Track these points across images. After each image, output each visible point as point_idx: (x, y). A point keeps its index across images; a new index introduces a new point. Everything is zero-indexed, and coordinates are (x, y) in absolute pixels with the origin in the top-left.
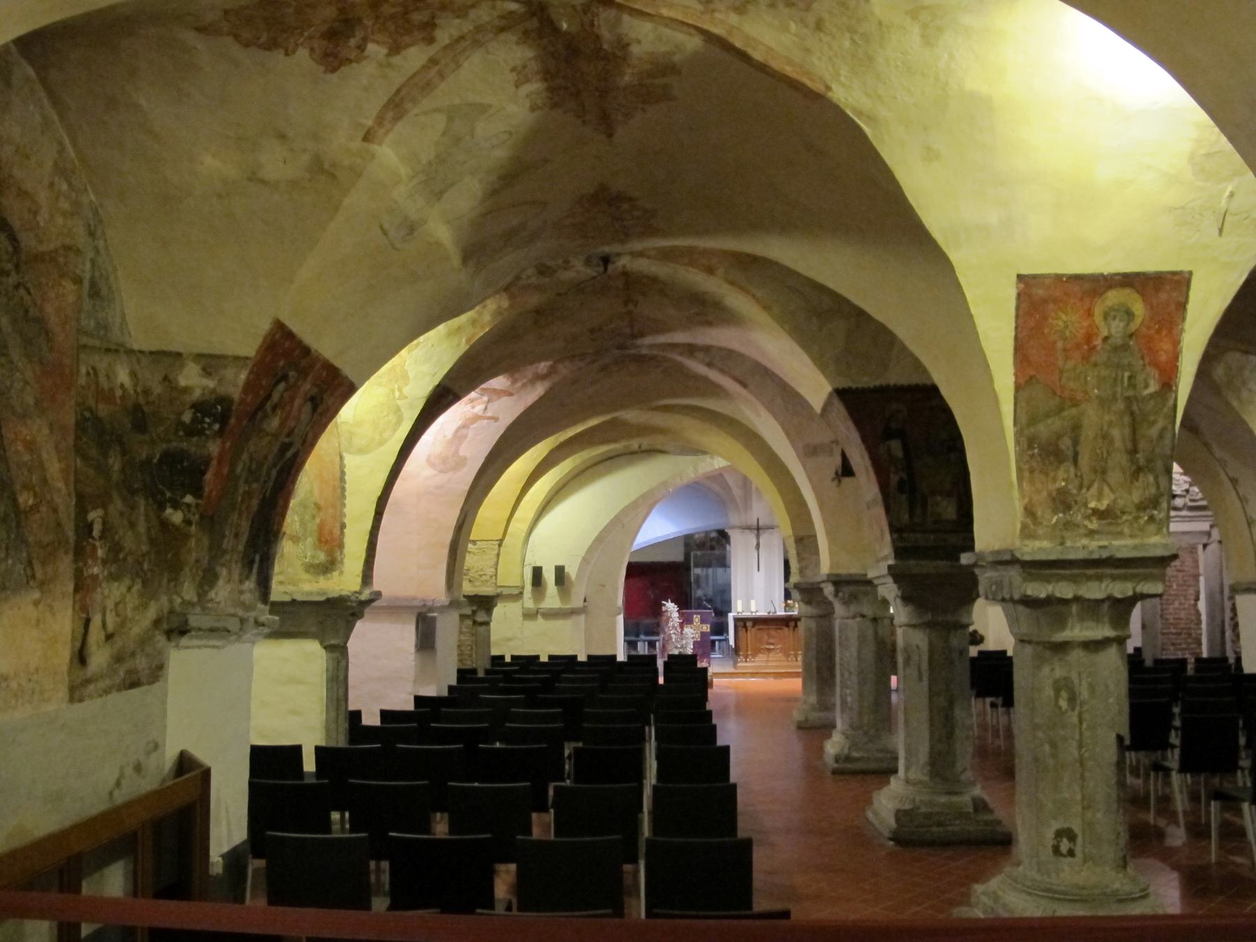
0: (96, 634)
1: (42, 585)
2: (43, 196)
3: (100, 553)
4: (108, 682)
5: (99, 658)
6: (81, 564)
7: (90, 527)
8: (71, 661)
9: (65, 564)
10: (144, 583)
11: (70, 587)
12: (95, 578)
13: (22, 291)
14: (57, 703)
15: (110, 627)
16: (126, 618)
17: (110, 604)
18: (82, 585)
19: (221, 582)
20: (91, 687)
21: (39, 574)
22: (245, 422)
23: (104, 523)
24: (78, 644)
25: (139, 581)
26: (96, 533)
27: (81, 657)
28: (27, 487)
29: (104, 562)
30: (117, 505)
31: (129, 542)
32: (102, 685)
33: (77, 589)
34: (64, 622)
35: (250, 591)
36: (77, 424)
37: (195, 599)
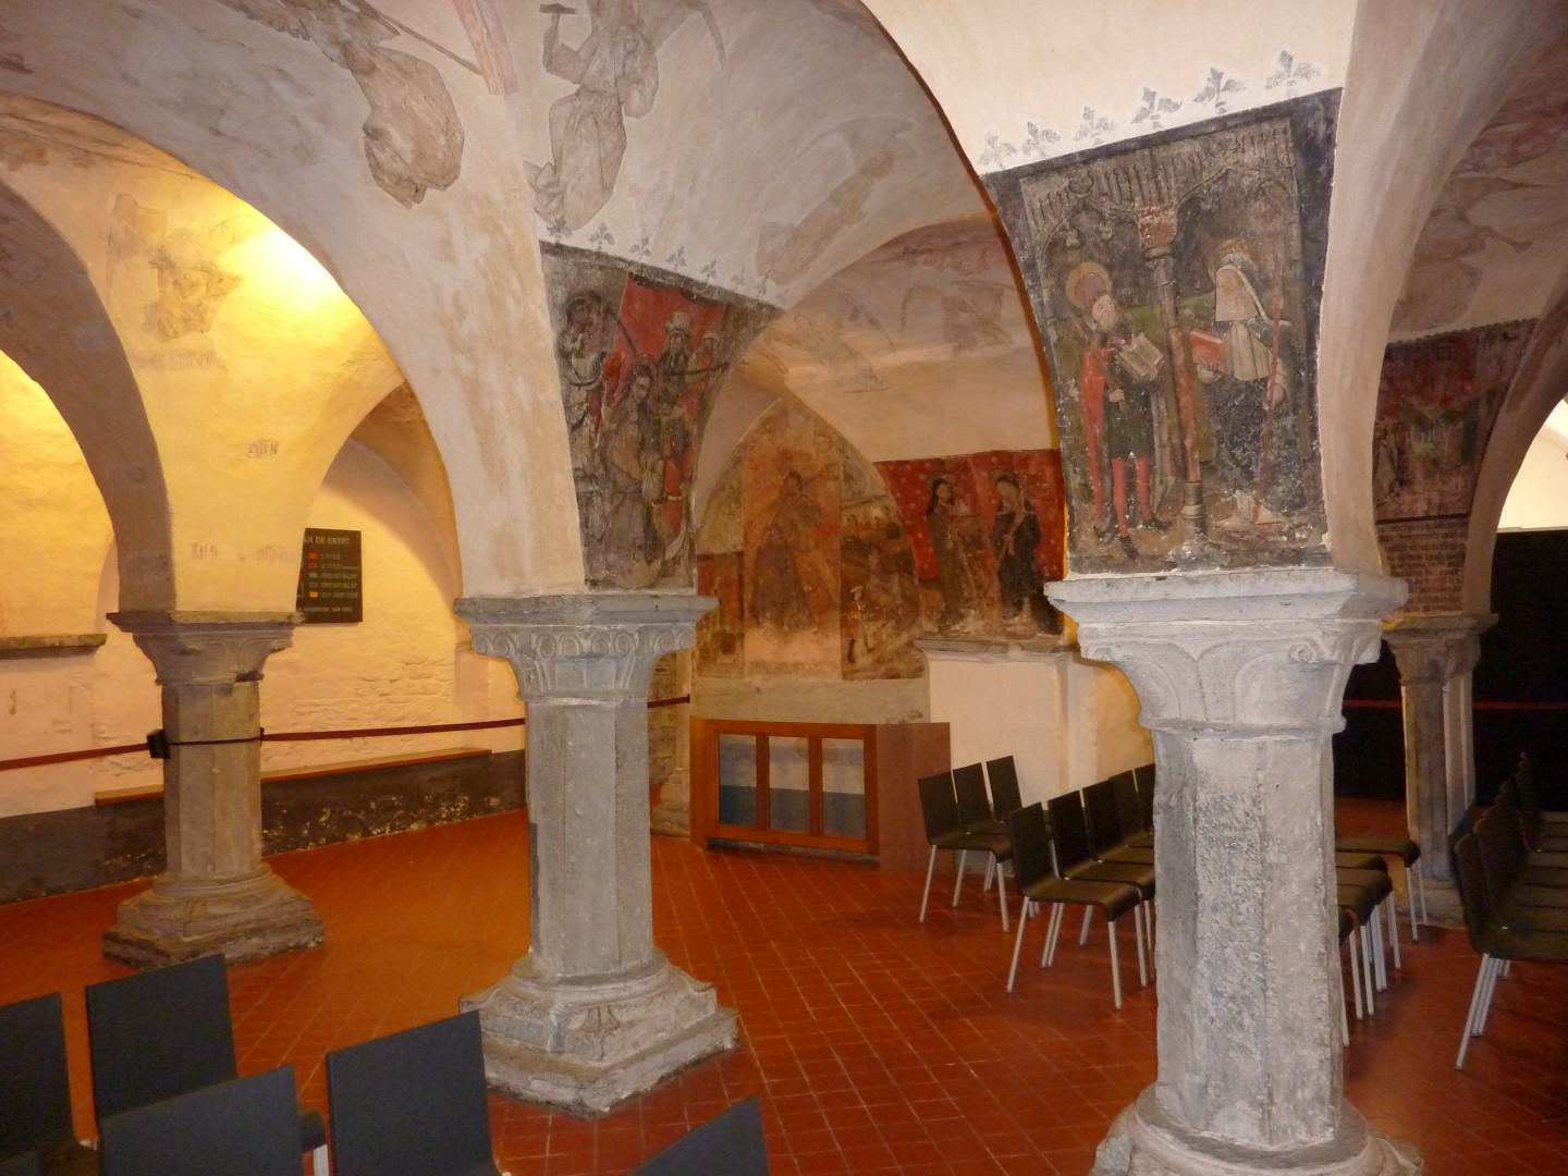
0: (859, 648)
1: (819, 625)
2: (812, 451)
3: (859, 608)
4: (871, 673)
5: (863, 660)
6: (845, 614)
7: (853, 595)
8: (843, 659)
9: (836, 615)
10: (899, 622)
11: (838, 625)
12: (856, 621)
13: (804, 499)
14: (835, 677)
15: (871, 645)
16: (882, 641)
17: (869, 633)
18: (845, 624)
19: (970, 619)
20: (858, 674)
21: (816, 619)
22: (925, 518)
23: (863, 592)
24: (847, 652)
25: (893, 622)
26: (856, 598)
27: (850, 657)
28: (809, 583)
29: (863, 612)
30: (874, 580)
31: (884, 599)
32: (866, 674)
33: (842, 626)
34: (835, 642)
35: (1024, 624)
36: (842, 547)
37: (936, 630)
